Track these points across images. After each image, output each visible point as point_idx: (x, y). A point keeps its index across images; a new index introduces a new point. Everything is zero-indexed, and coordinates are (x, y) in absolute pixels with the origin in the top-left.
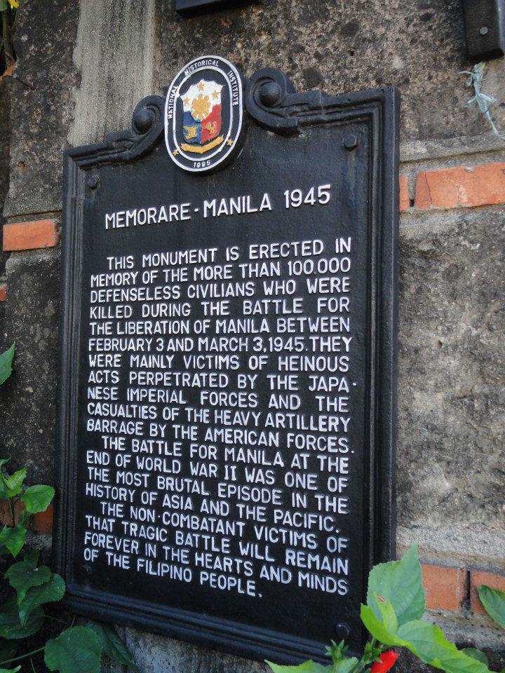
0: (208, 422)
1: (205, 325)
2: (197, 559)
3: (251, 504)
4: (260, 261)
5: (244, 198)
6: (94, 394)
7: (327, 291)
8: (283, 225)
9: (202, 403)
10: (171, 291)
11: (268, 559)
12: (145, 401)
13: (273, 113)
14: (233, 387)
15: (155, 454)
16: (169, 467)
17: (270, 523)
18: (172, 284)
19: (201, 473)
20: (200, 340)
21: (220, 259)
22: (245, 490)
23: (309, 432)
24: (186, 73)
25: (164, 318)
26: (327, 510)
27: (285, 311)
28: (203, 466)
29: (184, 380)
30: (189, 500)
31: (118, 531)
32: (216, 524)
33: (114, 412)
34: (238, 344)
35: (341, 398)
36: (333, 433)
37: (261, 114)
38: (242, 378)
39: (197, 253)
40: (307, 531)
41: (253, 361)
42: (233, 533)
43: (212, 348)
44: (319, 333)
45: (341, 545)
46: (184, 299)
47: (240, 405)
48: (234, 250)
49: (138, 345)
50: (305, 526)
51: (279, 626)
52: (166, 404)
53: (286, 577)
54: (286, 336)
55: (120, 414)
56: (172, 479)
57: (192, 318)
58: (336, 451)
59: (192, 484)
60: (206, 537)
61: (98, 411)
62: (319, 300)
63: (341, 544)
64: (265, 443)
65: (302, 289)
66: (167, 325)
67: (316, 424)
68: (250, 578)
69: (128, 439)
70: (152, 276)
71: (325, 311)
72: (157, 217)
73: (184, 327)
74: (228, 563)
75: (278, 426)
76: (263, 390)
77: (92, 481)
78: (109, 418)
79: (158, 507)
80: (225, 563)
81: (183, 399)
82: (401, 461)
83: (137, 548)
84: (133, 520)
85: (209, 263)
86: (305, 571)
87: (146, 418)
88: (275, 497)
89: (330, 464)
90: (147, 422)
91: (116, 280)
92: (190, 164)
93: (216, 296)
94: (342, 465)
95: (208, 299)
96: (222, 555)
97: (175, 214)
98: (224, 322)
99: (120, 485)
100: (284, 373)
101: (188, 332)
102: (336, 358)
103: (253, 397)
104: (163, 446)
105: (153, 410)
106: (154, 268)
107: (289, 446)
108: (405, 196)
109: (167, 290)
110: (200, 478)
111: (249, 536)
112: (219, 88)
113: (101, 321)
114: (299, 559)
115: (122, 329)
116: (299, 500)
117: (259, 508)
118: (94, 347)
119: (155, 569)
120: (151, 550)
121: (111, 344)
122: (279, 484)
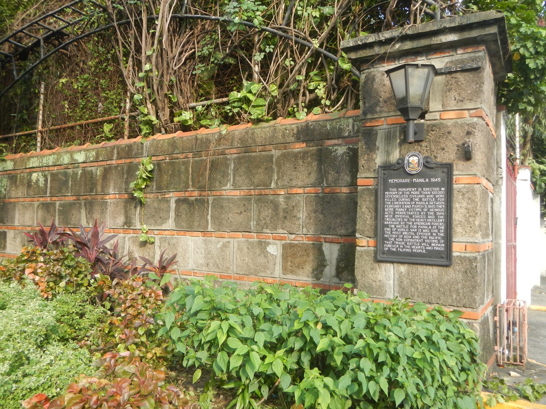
1: (414, 203)
3: (424, 236)
6: (386, 216)
8: (430, 185)
12: (400, 217)
14: (420, 214)
17: (428, 239)
21: (417, 190)
37: (426, 164)
46: (409, 197)
51: (430, 257)
54: (431, 205)
57: (411, 201)
61: (388, 219)
63: (443, 241)
65: (435, 197)
69: (395, 225)
70: (401, 193)
73: (409, 203)
74: (419, 247)
76: (427, 215)
79: (403, 238)
82: (453, 227)
91: (392, 193)
94: (443, 228)
100: (431, 212)
108: (454, 181)
111: (424, 242)
116: (434, 234)
120: (401, 246)
121: (390, 206)
122: (430, 232)
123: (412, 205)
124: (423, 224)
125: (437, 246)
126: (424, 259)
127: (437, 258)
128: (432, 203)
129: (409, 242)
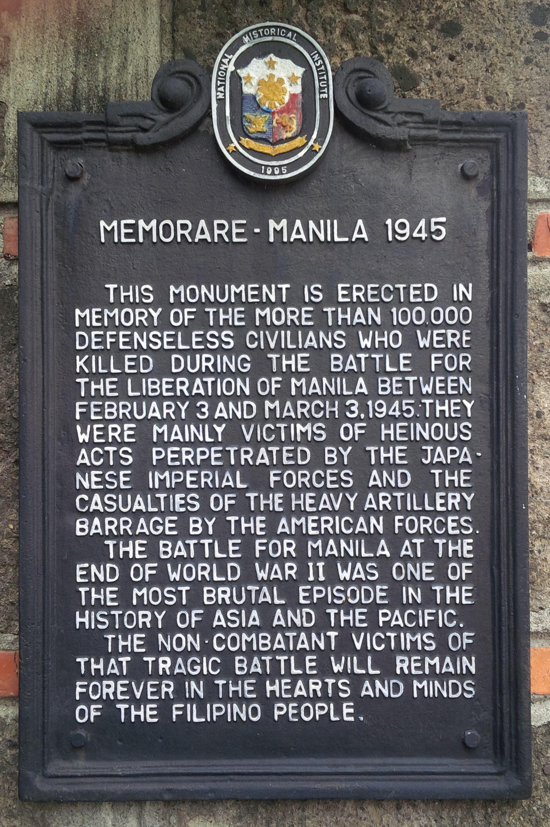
0: (281, 509)
2: (269, 688)
3: (347, 607)
4: (353, 305)
5: (329, 222)
7: (443, 346)
8: (383, 261)
9: (272, 485)
10: (219, 338)
11: (371, 672)
12: (181, 487)
13: (376, 119)
14: (318, 461)
15: (200, 556)
16: (222, 571)
18: (220, 329)
19: (273, 576)
20: (268, 404)
21: (295, 299)
22: (338, 591)
23: (424, 512)
24: (246, 39)
25: (208, 372)
26: (448, 602)
27: (389, 369)
28: (276, 566)
29: (243, 457)
30: (254, 613)
31: (138, 671)
32: (296, 638)
33: (125, 505)
34: (324, 409)
35: (462, 471)
36: (454, 511)
37: (353, 114)
38: (331, 452)
39: (260, 289)
40: (423, 629)
41: (346, 429)
42: (322, 646)
43: (285, 414)
44: (434, 395)
45: (466, 641)
47: (329, 486)
48: (316, 289)
49: (165, 411)
50: (421, 625)
51: (388, 750)
52: (214, 490)
53: (396, 688)
55: (136, 507)
56: (228, 589)
58: (457, 532)
59: (258, 592)
60: (283, 658)
62: (433, 356)
63: (466, 639)
64: (365, 530)
65: (411, 342)
66: (214, 383)
67: (433, 503)
68: (346, 700)
69: (152, 543)
70: (186, 316)
71: (441, 368)
72: (193, 234)
73: (242, 386)
75: (381, 508)
76: (361, 465)
77: (89, 606)
78: (118, 514)
79: (205, 628)
80: (312, 687)
81: (242, 482)
83: (170, 690)
84: (164, 652)
85: (279, 302)
86: (420, 678)
87: (183, 510)
88: (379, 594)
89: (451, 548)
90: (184, 517)
92: (257, 167)
93: (290, 346)
94: (466, 547)
95: (278, 349)
96: (306, 677)
97: (223, 233)
98: (303, 380)
99: (141, 605)
100: (389, 443)
101: (247, 392)
102: (456, 424)
103: (346, 475)
104: (211, 546)
105: (193, 498)
106: (192, 305)
107: (397, 531)
109: (212, 336)
110: (270, 583)
111: (345, 645)
112: (299, 71)
113: (96, 377)
114: (413, 665)
115: (137, 387)
116: (411, 593)
117: (358, 611)
118: (85, 416)
119: (202, 712)
120: (195, 688)
121: (113, 410)
122: (386, 577)
123: (260, 400)
124: (341, 524)
125: (433, 675)
126: (351, 764)
127: (431, 751)
128: (392, 386)
129: (250, 653)
